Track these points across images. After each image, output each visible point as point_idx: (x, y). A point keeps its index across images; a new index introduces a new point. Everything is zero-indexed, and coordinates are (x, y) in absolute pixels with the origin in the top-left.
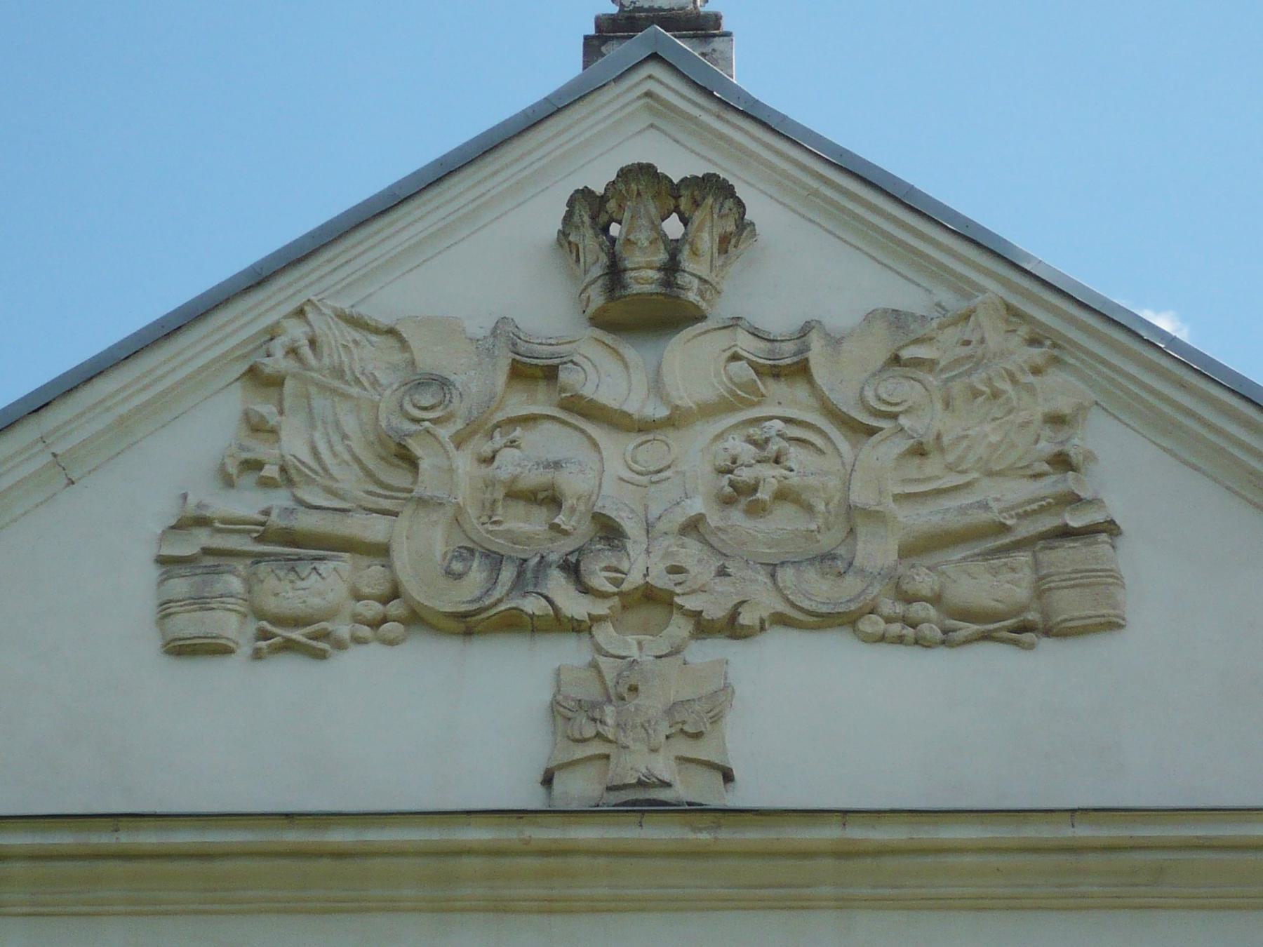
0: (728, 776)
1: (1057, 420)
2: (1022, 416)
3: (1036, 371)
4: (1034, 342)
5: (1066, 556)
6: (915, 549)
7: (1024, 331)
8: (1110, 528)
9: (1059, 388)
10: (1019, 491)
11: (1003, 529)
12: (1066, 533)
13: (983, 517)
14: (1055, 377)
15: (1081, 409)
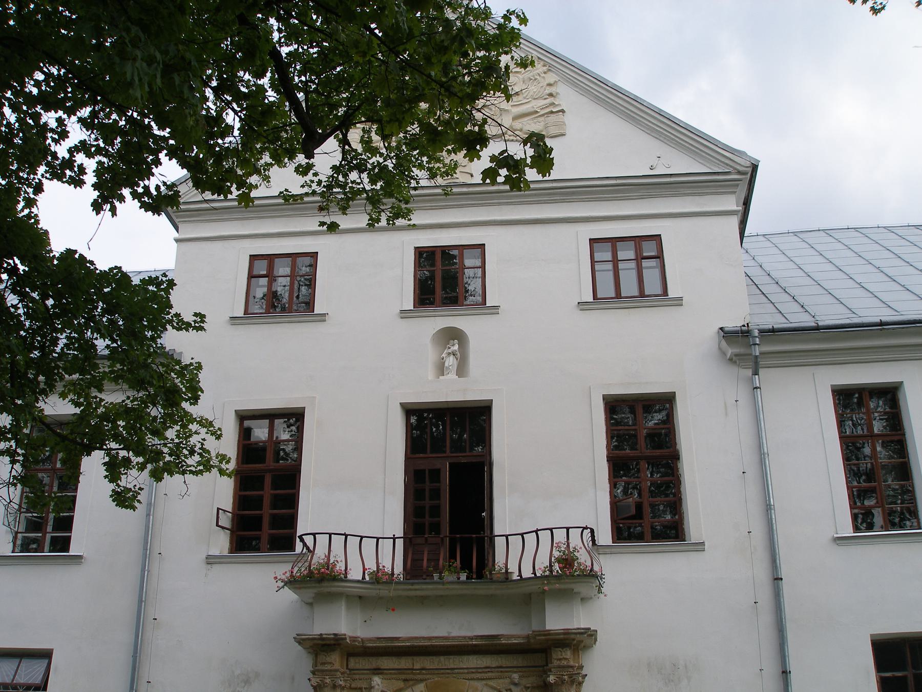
0: (472, 176)
1: (550, 85)
2: (541, 85)
3: (545, 73)
4: (544, 66)
5: (553, 118)
6: (516, 118)
7: (542, 63)
8: (563, 111)
9: (551, 77)
10: (542, 103)
11: (537, 112)
12: (552, 112)
13: (532, 110)
14: (550, 74)
15: (556, 82)
